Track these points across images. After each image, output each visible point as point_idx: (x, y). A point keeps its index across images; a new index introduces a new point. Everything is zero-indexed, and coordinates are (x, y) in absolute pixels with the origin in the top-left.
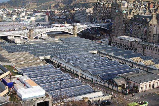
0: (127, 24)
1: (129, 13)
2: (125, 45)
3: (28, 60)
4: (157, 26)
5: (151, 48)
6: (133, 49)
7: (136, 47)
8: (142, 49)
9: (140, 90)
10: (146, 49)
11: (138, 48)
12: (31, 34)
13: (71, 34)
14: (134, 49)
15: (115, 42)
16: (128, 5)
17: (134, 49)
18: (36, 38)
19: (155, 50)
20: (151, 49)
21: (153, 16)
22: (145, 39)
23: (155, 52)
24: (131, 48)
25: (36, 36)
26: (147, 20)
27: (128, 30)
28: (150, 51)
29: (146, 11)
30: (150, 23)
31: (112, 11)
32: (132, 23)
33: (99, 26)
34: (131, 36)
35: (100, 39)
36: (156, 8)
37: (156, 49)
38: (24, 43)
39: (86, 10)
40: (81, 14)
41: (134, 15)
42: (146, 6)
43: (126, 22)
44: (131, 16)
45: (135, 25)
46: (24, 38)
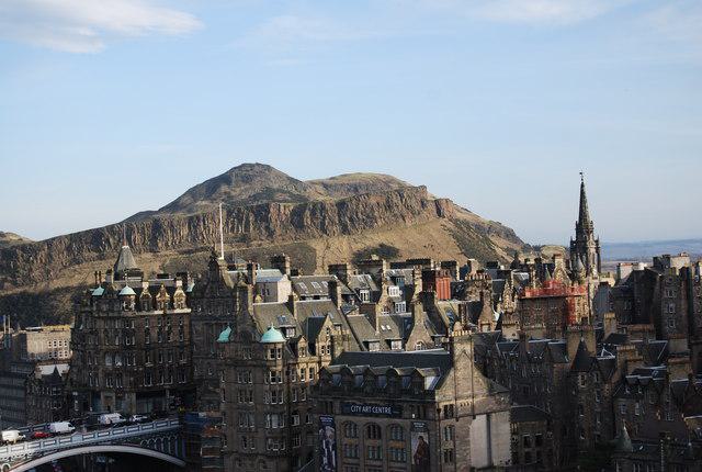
0: (295, 413)
1: (302, 343)
4: (488, 416)
16: (294, 288)
21: (458, 348)
26: (423, 378)
27: (310, 455)
29: (411, 320)
30: (444, 398)
31: (196, 339)
32: (327, 409)
36: (474, 298)
39: (23, 338)
41: (338, 353)
42: (408, 291)
43: (289, 403)
44: (320, 363)
45: (351, 418)
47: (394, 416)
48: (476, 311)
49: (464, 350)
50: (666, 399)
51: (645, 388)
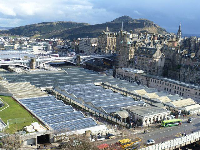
2: (130, 77)
3: (29, 91)
5: (156, 81)
6: (137, 81)
7: (140, 80)
8: (147, 81)
9: (144, 123)
10: (150, 82)
11: (142, 80)
12: (33, 63)
13: (74, 65)
14: (138, 81)
15: (119, 74)
17: (138, 81)
18: (38, 68)
19: (159, 82)
20: (156, 82)
21: (158, 48)
22: (150, 71)
23: (159, 84)
24: (135, 80)
25: (39, 66)
28: (154, 83)
33: (103, 57)
34: (136, 68)
35: (104, 71)
37: (161, 82)
38: (25, 73)
40: (85, 44)
46: (25, 68)
47: (146, 57)
48: (161, 43)
49: (159, 48)
50: (190, 59)
51: (187, 57)
